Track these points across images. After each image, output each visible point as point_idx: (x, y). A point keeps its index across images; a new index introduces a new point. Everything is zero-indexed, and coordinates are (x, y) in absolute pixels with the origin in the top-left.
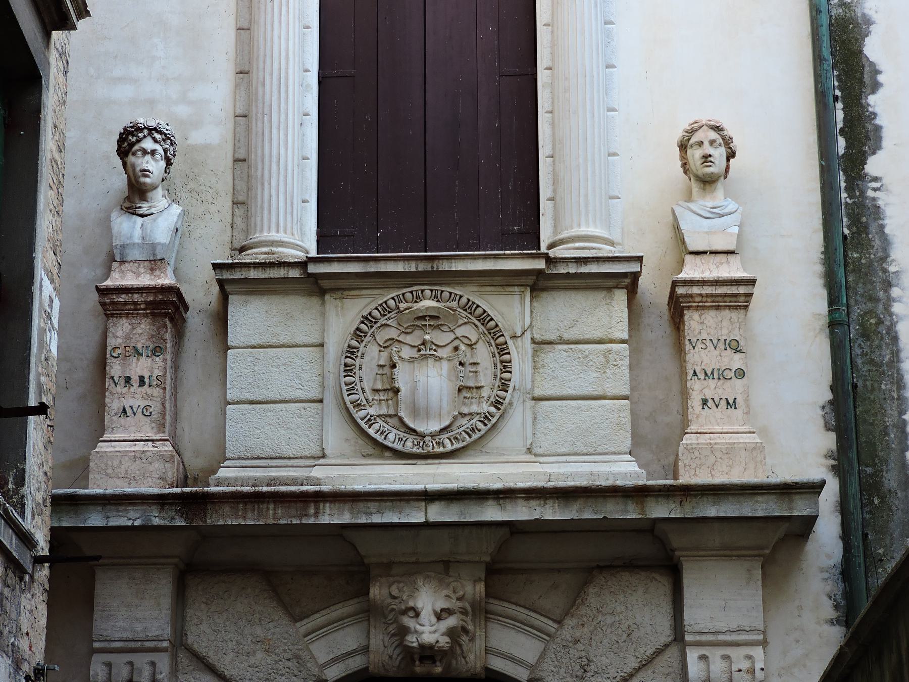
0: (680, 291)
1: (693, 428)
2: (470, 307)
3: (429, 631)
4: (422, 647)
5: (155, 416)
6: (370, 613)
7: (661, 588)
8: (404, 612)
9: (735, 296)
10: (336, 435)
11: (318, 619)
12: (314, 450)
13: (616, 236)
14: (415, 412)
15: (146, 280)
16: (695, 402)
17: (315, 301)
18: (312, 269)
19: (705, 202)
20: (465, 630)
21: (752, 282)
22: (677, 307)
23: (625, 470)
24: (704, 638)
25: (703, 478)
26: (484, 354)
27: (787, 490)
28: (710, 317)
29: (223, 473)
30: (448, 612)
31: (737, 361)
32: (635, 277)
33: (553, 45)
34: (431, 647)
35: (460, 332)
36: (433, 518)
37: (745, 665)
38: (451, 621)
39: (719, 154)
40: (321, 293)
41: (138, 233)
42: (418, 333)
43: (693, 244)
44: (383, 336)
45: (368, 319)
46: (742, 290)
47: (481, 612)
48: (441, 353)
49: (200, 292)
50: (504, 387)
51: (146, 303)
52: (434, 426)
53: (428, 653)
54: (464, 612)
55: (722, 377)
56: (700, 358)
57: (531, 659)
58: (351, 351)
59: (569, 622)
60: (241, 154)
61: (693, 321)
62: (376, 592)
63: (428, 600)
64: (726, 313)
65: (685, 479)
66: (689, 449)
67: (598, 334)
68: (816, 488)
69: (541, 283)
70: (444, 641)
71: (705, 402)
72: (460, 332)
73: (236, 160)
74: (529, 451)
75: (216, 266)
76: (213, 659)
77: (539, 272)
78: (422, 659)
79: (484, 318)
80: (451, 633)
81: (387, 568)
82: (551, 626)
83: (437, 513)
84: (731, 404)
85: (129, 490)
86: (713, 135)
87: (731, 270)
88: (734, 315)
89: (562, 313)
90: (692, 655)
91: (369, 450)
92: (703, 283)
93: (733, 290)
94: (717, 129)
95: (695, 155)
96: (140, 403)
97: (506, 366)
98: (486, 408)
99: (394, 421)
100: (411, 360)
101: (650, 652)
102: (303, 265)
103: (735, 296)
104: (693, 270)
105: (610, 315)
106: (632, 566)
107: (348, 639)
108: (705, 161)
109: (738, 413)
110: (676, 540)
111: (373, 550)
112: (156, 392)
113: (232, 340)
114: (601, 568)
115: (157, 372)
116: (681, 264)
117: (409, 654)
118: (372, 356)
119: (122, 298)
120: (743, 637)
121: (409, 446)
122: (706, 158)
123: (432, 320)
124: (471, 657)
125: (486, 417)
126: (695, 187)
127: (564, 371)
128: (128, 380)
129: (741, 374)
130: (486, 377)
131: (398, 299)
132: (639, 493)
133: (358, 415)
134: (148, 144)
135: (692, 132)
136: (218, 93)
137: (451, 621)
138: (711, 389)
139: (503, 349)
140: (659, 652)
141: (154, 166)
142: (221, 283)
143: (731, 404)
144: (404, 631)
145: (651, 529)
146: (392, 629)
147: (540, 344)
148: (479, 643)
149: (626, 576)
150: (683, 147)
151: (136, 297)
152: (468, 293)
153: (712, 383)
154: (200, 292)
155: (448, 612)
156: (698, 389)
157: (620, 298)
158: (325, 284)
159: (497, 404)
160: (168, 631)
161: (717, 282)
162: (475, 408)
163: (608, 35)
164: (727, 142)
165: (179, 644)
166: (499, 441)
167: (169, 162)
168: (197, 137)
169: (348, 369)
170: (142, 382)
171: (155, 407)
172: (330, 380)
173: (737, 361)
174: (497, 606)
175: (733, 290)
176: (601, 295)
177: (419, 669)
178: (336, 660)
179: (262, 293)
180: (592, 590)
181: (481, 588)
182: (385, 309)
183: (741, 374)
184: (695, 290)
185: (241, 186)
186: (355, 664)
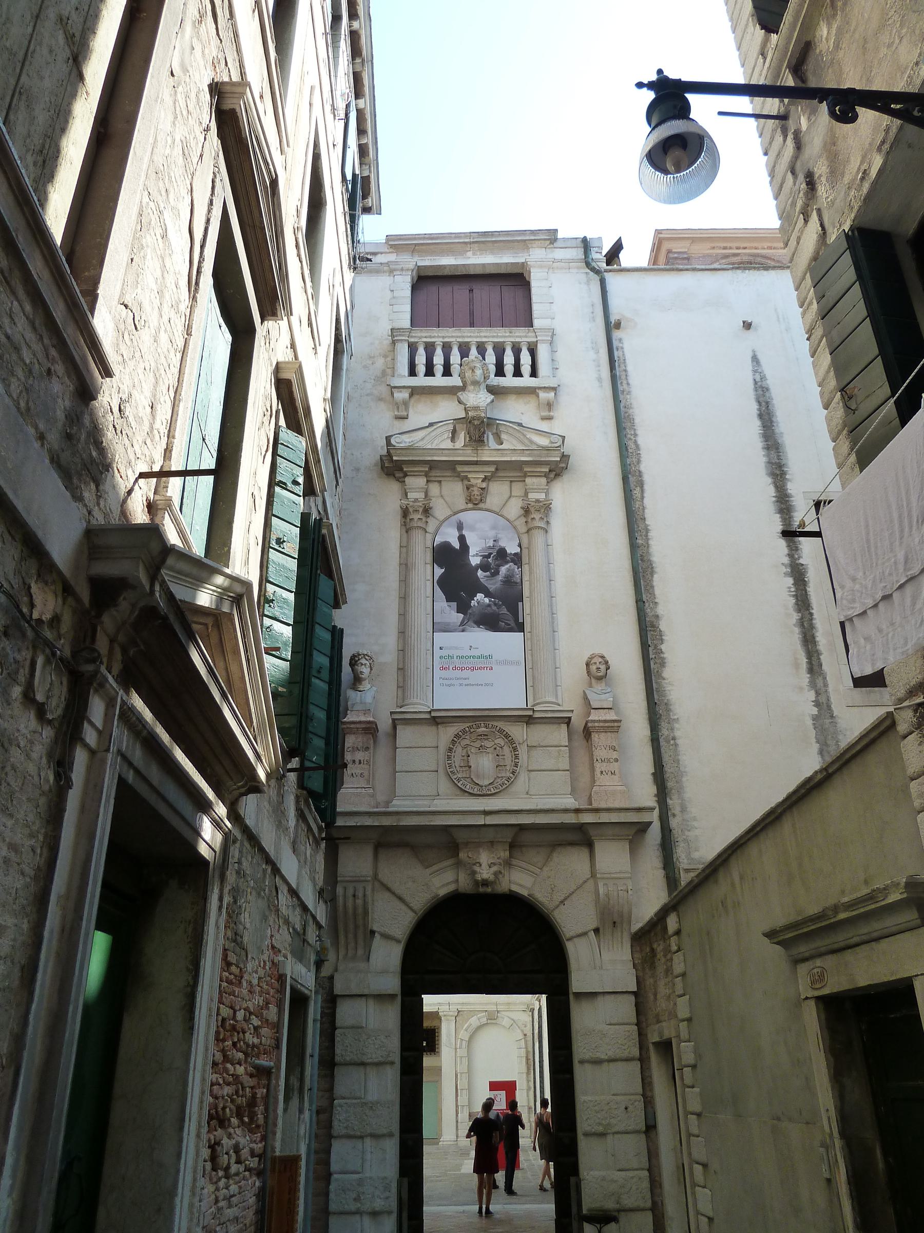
0: (590, 725)
1: (597, 783)
2: (501, 731)
3: (485, 873)
4: (483, 880)
5: (366, 777)
6: (459, 864)
7: (584, 853)
8: (474, 864)
9: (613, 727)
10: (444, 786)
11: (435, 868)
12: (435, 793)
13: (560, 702)
14: (478, 776)
15: (363, 718)
16: (598, 772)
17: (434, 728)
18: (433, 714)
19: (599, 687)
20: (500, 872)
21: (620, 721)
22: (587, 733)
23: (570, 802)
24: (605, 876)
25: (603, 805)
26: (507, 750)
27: (639, 810)
28: (602, 735)
29: (394, 802)
30: (494, 864)
31: (615, 755)
32: (570, 718)
33: (531, 622)
34: (486, 880)
35: (496, 741)
36: (487, 823)
37: (624, 888)
38: (495, 869)
39: (603, 667)
40: (437, 724)
41: (358, 698)
42: (479, 741)
43: (594, 705)
44: (464, 742)
45: (457, 736)
46: (616, 724)
47: (508, 864)
48: (488, 750)
49: (384, 724)
50: (516, 765)
51: (364, 729)
52: (487, 783)
53: (485, 883)
54: (500, 864)
55: (609, 761)
56: (600, 753)
57: (529, 885)
58: (450, 750)
59: (544, 868)
60: (401, 666)
61: (595, 736)
62: (462, 855)
63: (485, 857)
64: (609, 734)
65: (595, 805)
66: (596, 793)
67: (555, 743)
68: (652, 809)
69: (531, 721)
70: (492, 878)
71: (602, 772)
72: (496, 741)
73: (398, 669)
74: (527, 793)
75: (391, 713)
76: (389, 885)
77: (530, 716)
78: (483, 885)
79: (507, 736)
80: (495, 874)
81: (467, 844)
82: (537, 871)
83: (490, 820)
84: (613, 773)
85: (355, 809)
86: (600, 660)
87: (611, 716)
88: (613, 735)
89: (539, 734)
90: (601, 885)
91: (458, 792)
92: (600, 721)
93: (612, 724)
94: (603, 657)
95: (593, 668)
96: (359, 771)
97: (517, 757)
98: (509, 774)
99: (469, 780)
100: (476, 754)
101: (581, 882)
102: (430, 712)
103: (613, 727)
104: (595, 716)
105: (560, 735)
106: (572, 844)
107: (449, 876)
108: (598, 671)
109: (616, 777)
110: (592, 832)
111: (461, 836)
112: (366, 767)
113: (399, 743)
114: (560, 845)
115: (366, 758)
116: (589, 714)
117: (477, 883)
118: (459, 751)
119: (352, 726)
120: (622, 875)
121: (476, 791)
122: (598, 668)
123: (484, 736)
124: (503, 884)
125: (508, 779)
126: (593, 680)
127: (541, 759)
128: (354, 761)
129: (616, 760)
130: (508, 761)
131: (469, 727)
132: (577, 811)
133: (454, 777)
134: (363, 661)
135: (591, 658)
136: (391, 641)
137: (495, 869)
138: (604, 767)
139: (515, 749)
140: (585, 882)
141: (365, 670)
142: (394, 720)
143: (613, 773)
144: (474, 873)
145: (581, 828)
146: (469, 872)
147: (530, 747)
148: (507, 878)
149: (569, 848)
150: (588, 665)
151: (358, 726)
152: (500, 724)
153: (605, 764)
154: (384, 724)
155: (494, 864)
156: (599, 767)
157: (564, 726)
158: (438, 720)
159: (513, 773)
160: (371, 873)
161: (605, 721)
162: (503, 775)
163: (553, 618)
164: (607, 663)
165: (376, 877)
166: (513, 789)
167: (371, 669)
168: (382, 659)
169: (449, 758)
170: (360, 763)
171: (366, 774)
172: (441, 763)
173: (615, 755)
174: (514, 862)
175: (612, 724)
176: (555, 726)
177: (481, 890)
178: (443, 886)
179: (415, 724)
180: (555, 855)
181: (507, 853)
182: (464, 731)
183: (616, 760)
184: (596, 724)
185: (401, 679)
186: (451, 888)
